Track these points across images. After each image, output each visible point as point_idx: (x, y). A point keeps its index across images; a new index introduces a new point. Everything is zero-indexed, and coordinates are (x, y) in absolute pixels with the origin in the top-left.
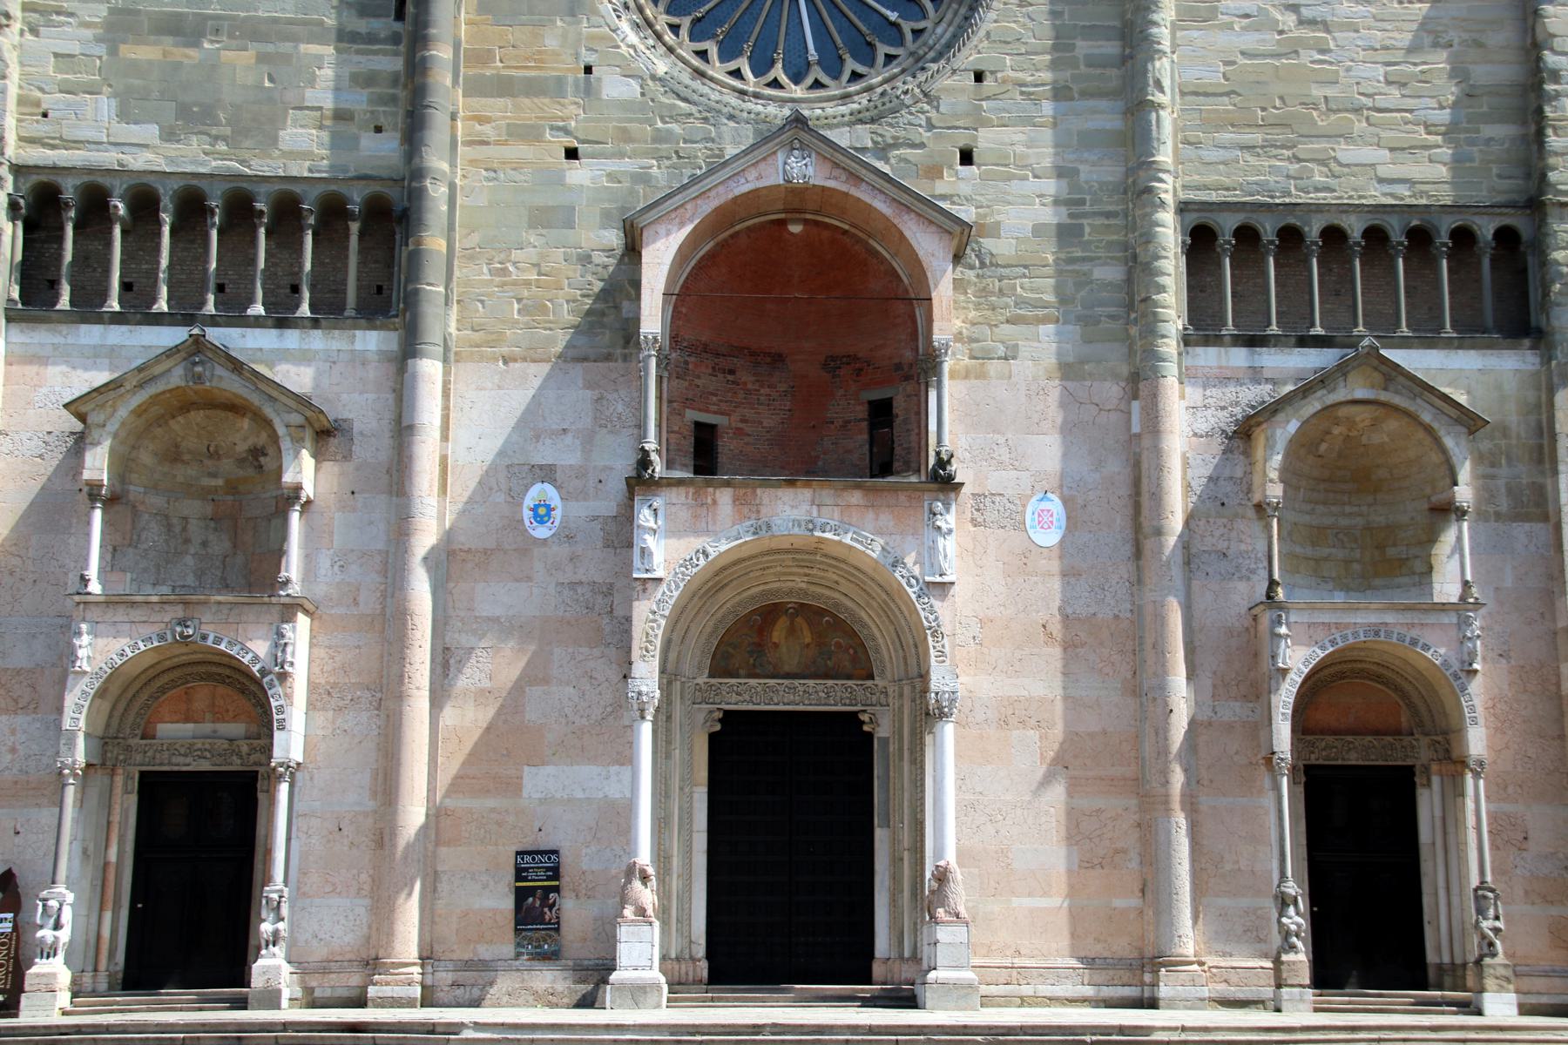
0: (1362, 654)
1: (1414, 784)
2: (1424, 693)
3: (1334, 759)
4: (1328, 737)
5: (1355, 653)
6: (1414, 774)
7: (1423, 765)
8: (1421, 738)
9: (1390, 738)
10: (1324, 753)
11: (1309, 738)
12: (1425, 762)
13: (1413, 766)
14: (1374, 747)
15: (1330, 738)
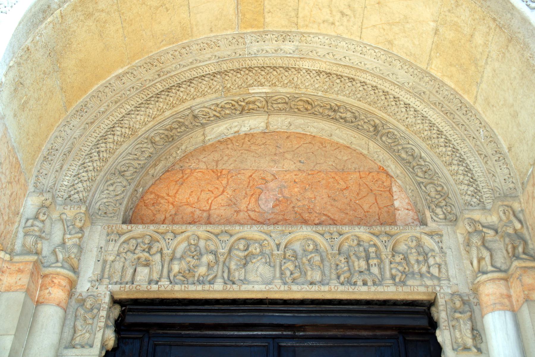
0: (288, 47)
1: (439, 349)
2: (446, 129)
3: (200, 282)
4: (192, 229)
5: (269, 47)
6: (434, 325)
7: (453, 294)
8: (446, 230)
9: (362, 233)
10: (176, 268)
11: (139, 229)
12: (464, 289)
13: (431, 304)
14: (316, 250)
15: (201, 231)
